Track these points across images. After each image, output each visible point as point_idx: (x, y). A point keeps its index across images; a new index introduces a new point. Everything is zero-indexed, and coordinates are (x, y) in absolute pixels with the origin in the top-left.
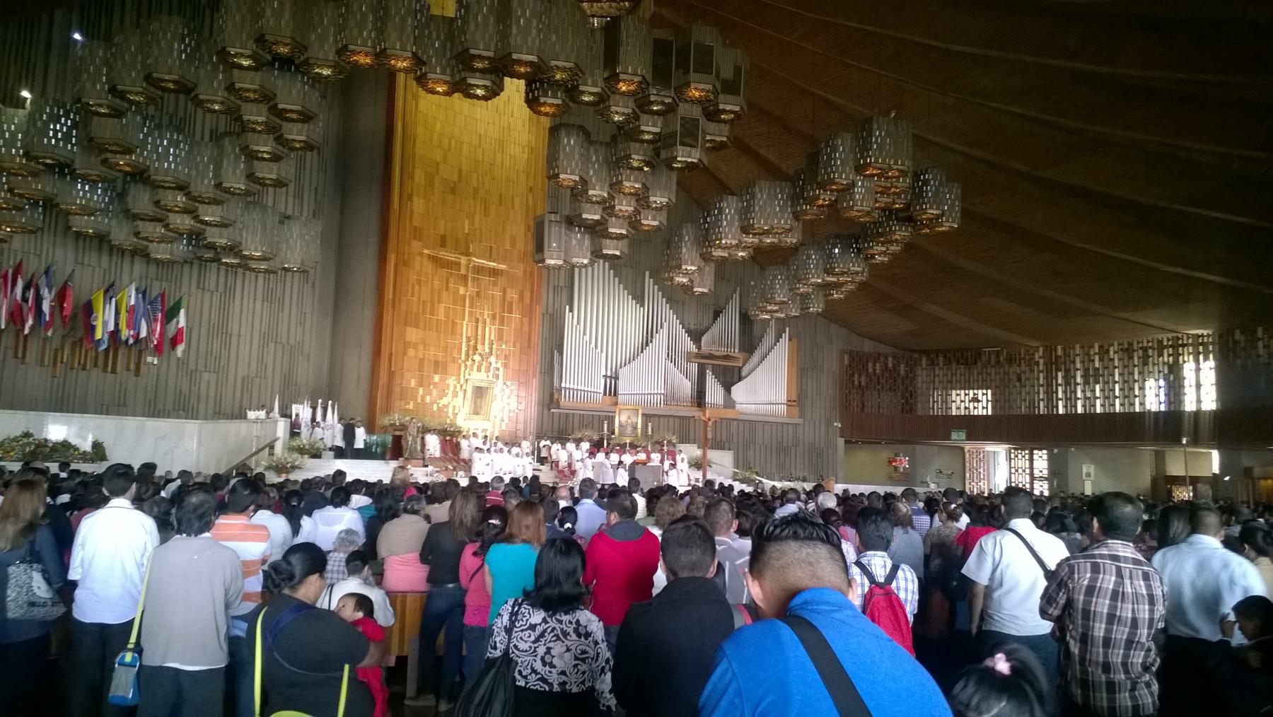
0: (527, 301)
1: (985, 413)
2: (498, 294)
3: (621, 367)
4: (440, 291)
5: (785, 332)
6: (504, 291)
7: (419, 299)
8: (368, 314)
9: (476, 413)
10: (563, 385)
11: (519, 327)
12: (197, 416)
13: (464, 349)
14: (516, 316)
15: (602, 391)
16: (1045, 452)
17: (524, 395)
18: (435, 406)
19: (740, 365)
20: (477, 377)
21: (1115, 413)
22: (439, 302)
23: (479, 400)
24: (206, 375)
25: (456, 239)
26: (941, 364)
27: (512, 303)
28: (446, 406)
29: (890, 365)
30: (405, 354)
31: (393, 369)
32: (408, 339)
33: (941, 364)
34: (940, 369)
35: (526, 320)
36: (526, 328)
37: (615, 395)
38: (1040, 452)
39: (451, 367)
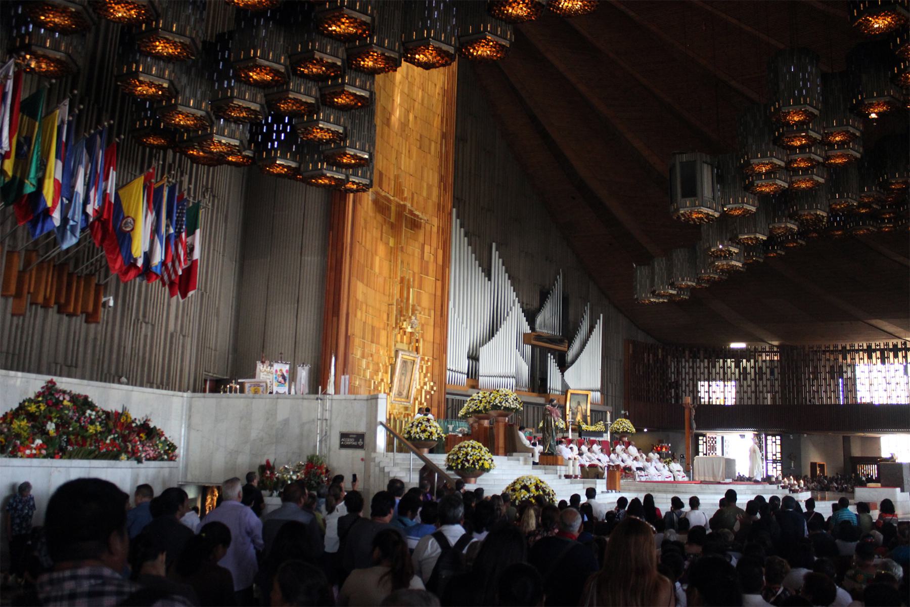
1: (749, 403)
2: (417, 252)
3: (480, 347)
5: (600, 319)
8: (312, 262)
11: (434, 293)
12: (168, 384)
15: (466, 372)
16: (778, 437)
19: (566, 349)
21: (839, 405)
25: (389, 178)
26: (702, 357)
27: (427, 262)
29: (660, 357)
30: (355, 316)
31: (349, 334)
32: (357, 297)
33: (702, 357)
34: (686, 361)
35: (439, 283)
37: (475, 378)
38: (774, 438)
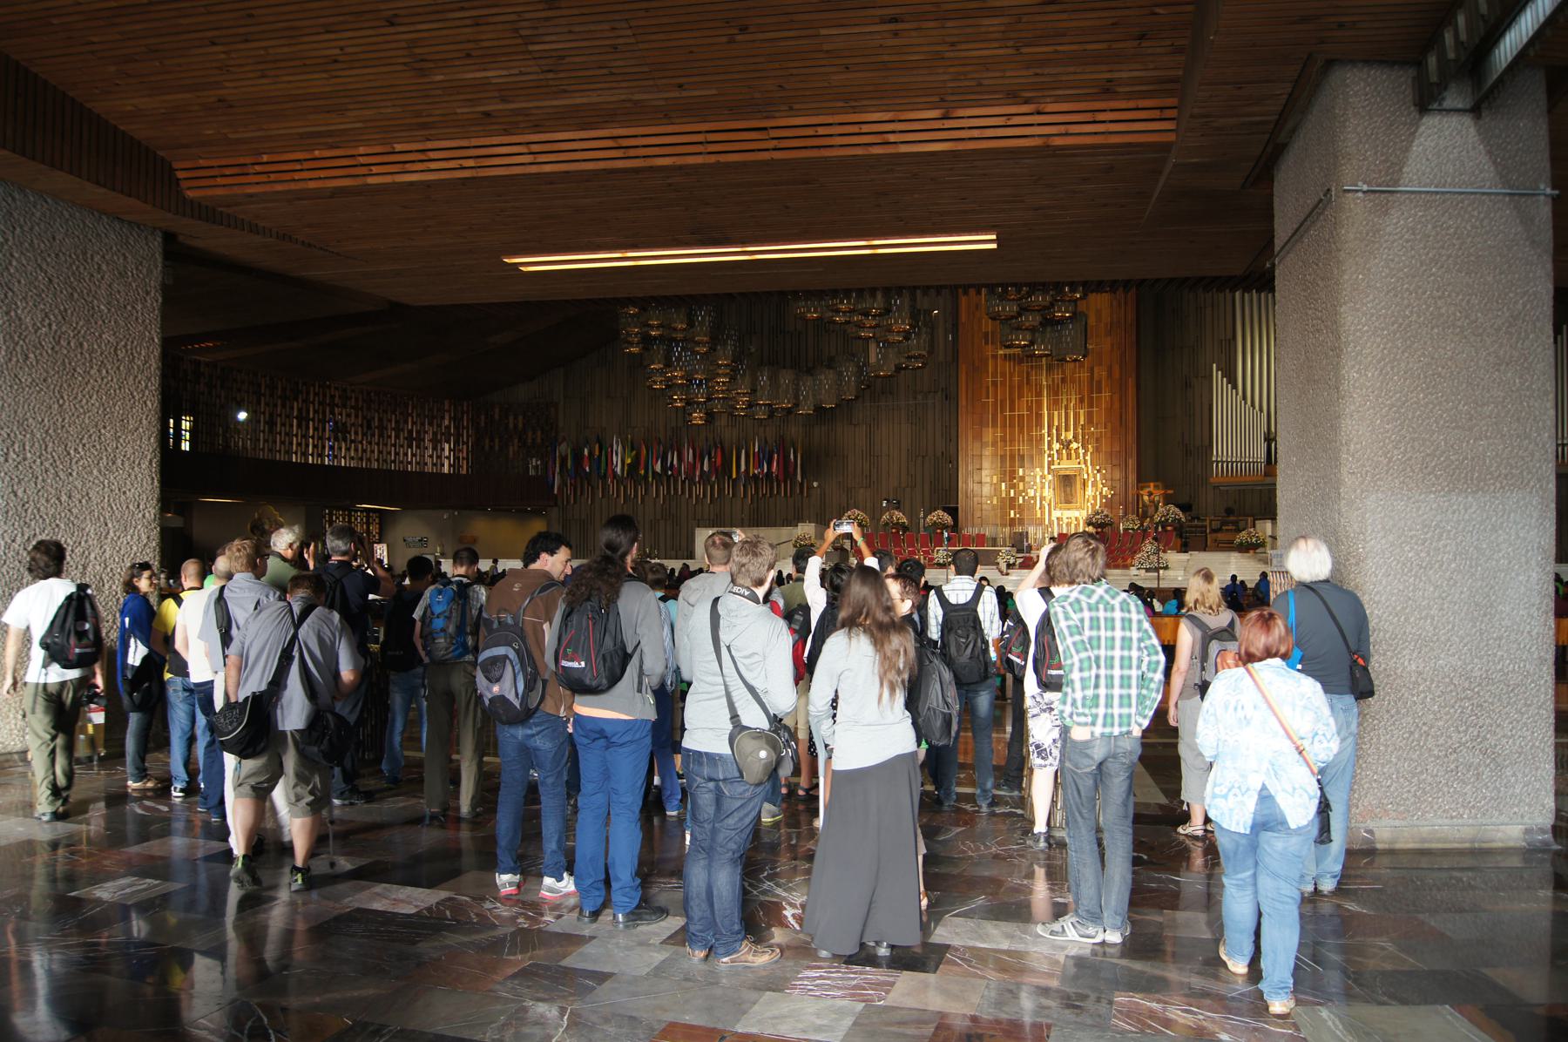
0: (1117, 376)
2: (1085, 375)
4: (1020, 387)
6: (1091, 370)
7: (997, 400)
9: (1068, 502)
10: (1214, 459)
13: (1046, 439)
14: (1105, 395)
17: (1118, 477)
18: (1021, 498)
20: (1067, 466)
22: (1021, 396)
23: (1068, 489)
24: (862, 491)
27: (1099, 382)
28: (1034, 498)
35: (1116, 397)
36: (1117, 405)
39: (1036, 459)
